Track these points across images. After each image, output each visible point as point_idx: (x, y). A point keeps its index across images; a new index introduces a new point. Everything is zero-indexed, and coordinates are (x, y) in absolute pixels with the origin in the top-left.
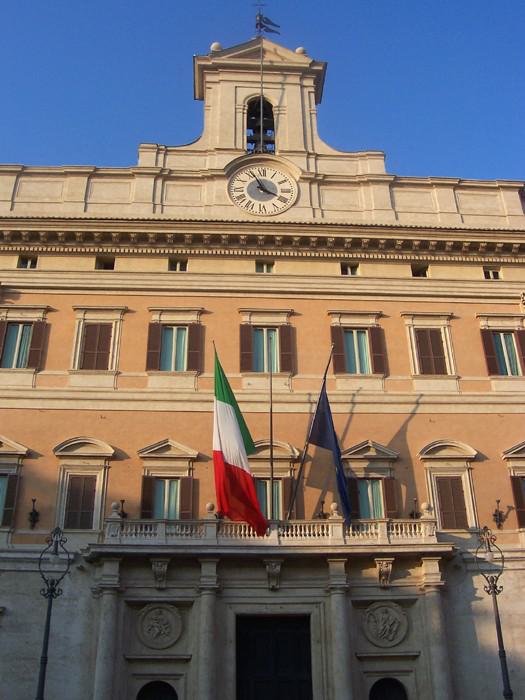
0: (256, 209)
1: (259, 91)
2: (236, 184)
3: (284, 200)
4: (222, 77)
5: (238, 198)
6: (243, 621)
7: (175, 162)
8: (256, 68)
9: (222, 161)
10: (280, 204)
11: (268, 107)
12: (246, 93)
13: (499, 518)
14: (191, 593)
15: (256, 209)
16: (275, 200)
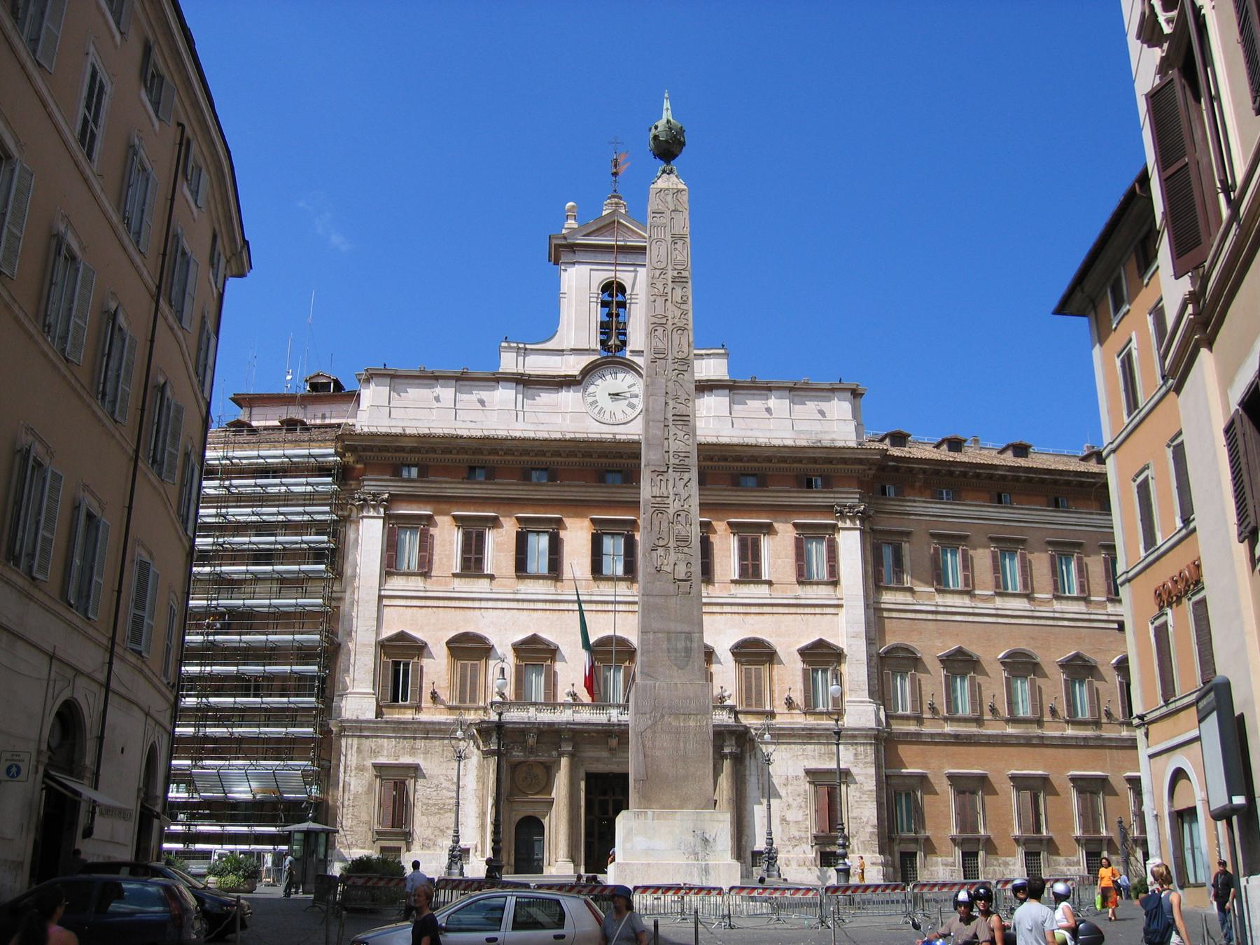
0: (607, 415)
1: (613, 274)
2: (591, 389)
3: (632, 406)
4: (579, 257)
5: (592, 404)
6: (591, 778)
7: (537, 365)
8: (612, 247)
9: (573, 365)
10: (628, 411)
11: (621, 289)
12: (602, 275)
13: (790, 703)
14: (554, 753)
15: (607, 415)
16: (623, 404)
